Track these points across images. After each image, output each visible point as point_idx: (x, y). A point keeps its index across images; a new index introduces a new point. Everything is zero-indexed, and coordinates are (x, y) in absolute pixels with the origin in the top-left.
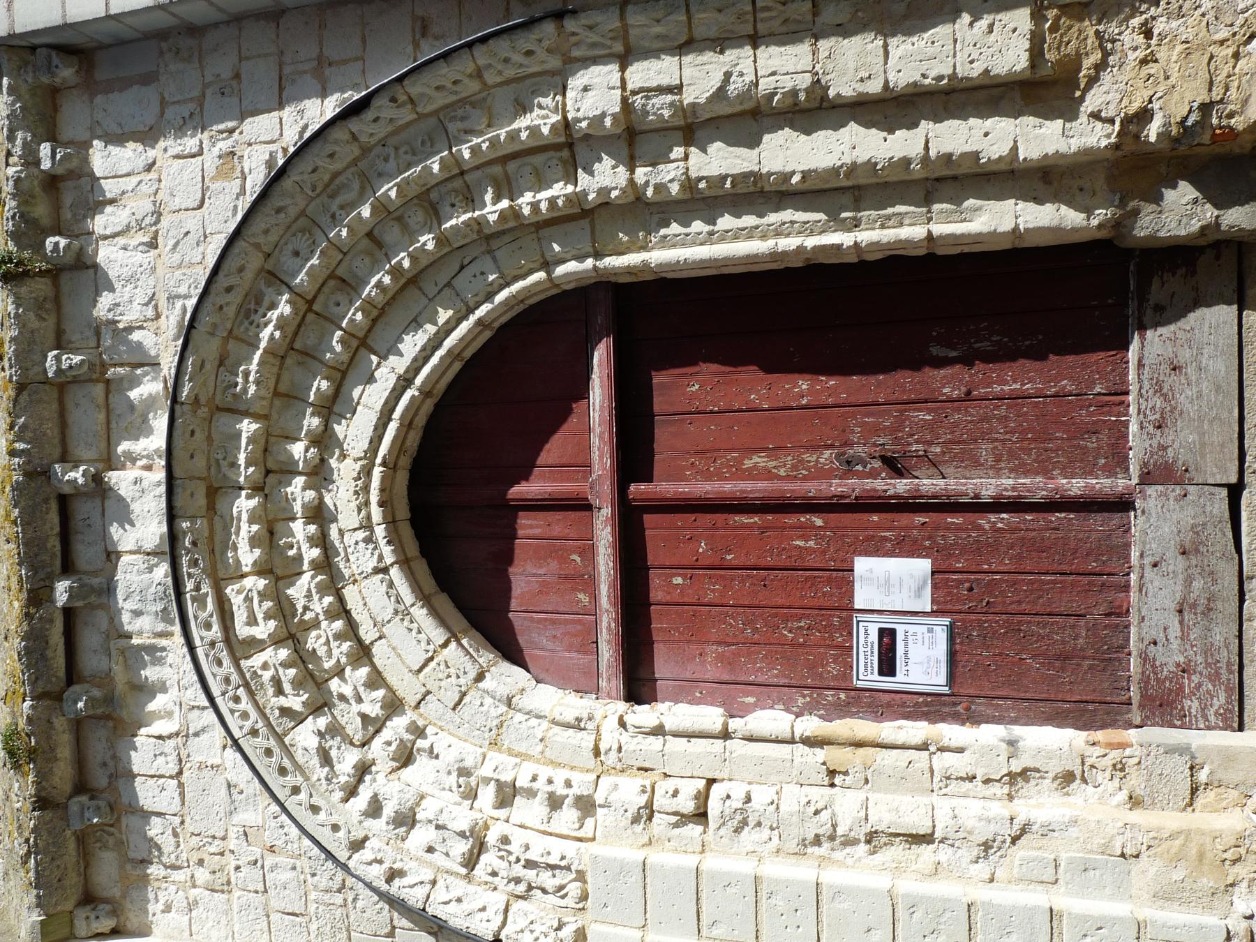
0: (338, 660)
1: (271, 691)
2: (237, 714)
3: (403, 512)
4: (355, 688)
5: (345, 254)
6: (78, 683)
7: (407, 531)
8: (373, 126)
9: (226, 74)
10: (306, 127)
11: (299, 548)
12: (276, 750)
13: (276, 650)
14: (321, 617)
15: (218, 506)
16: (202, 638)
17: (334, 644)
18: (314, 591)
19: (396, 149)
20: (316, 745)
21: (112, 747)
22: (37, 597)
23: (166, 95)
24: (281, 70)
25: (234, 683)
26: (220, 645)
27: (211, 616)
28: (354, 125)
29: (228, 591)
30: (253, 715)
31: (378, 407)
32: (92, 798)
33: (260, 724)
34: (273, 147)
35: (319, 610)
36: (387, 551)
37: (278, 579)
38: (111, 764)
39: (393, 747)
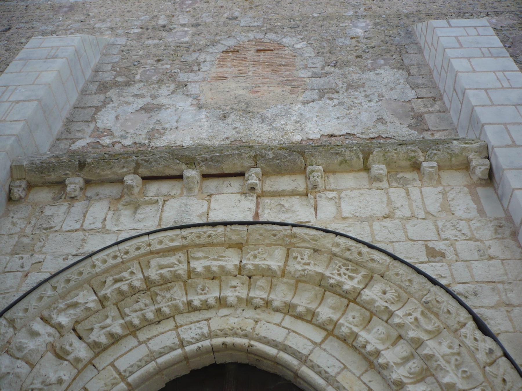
0: (128, 316)
1: (116, 277)
2: (106, 257)
3: (221, 359)
4: (110, 325)
5: (386, 322)
6: (143, 183)
7: (207, 361)
8: (472, 337)
9: (491, 252)
10: (466, 297)
11: (201, 294)
12: (80, 278)
13: (141, 279)
15: (230, 249)
16: (153, 240)
17: (139, 313)
18: (174, 302)
19: (459, 354)
20: (80, 301)
21: (106, 197)
23: (474, 222)
24: (499, 282)
26: (148, 249)
27: (166, 244)
28: (471, 324)
29: (180, 254)
30: (104, 266)
31: (287, 343)
32: (81, 189)
33: (98, 270)
34: (450, 278)
36: (194, 347)
37: (185, 282)
38: (97, 198)
39: (68, 347)
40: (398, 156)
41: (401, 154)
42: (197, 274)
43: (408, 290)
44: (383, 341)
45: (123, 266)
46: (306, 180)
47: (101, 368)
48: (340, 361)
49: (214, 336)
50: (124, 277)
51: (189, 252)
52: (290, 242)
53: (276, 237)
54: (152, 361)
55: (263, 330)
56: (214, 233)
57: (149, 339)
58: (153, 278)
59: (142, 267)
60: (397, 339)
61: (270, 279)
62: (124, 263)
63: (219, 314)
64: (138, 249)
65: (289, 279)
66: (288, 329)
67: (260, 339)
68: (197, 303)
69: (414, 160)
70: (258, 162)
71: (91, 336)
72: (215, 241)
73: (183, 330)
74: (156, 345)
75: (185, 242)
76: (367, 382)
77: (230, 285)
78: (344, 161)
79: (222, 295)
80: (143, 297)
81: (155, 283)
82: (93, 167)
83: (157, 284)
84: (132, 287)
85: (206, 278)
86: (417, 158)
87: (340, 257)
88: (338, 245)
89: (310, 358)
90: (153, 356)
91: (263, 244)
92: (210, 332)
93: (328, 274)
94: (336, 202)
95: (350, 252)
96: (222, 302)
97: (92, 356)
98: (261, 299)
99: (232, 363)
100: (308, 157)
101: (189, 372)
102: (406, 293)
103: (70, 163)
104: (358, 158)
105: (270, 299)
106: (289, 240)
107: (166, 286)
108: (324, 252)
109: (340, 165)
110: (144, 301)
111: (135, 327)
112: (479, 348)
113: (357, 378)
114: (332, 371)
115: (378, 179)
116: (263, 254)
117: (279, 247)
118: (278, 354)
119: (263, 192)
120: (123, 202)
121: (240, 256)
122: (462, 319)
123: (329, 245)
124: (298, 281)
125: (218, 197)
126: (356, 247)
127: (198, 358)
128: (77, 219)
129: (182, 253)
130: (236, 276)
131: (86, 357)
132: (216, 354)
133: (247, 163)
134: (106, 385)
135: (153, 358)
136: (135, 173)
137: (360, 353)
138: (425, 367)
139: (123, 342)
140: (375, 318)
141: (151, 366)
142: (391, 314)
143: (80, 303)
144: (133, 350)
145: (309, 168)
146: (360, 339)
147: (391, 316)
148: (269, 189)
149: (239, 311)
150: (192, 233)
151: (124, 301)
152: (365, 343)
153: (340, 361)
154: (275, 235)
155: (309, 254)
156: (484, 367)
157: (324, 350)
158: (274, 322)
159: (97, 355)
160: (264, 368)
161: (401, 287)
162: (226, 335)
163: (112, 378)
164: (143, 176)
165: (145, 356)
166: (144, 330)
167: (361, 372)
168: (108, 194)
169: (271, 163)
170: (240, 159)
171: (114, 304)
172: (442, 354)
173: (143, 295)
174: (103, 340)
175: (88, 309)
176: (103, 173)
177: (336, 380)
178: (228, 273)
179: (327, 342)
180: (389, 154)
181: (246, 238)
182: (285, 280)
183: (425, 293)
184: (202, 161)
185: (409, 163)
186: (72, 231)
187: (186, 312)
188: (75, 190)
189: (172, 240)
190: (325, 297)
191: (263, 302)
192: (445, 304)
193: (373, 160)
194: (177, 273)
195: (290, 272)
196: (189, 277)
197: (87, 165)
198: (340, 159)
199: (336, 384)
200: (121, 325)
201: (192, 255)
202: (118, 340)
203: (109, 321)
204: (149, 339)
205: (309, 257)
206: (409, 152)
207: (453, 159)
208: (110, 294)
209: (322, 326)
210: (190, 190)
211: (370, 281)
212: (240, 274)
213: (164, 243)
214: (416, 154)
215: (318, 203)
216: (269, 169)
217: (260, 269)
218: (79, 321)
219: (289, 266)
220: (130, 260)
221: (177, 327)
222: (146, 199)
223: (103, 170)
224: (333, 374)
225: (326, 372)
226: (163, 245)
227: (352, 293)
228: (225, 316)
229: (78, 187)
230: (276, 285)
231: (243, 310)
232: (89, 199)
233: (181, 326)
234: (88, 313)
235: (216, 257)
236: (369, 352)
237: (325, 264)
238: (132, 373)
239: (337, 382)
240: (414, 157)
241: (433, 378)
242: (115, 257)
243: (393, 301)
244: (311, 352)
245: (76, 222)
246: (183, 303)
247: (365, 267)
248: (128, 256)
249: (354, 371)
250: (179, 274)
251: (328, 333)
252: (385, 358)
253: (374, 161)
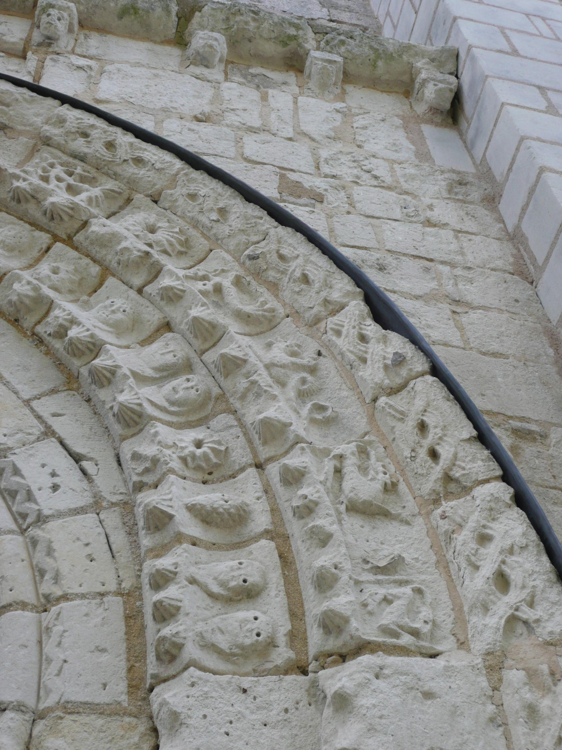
5: (140, 291)
8: (354, 333)
19: (313, 370)
24: (443, 263)
28: (357, 307)
40: (258, 28)
41: (266, 25)
44: (118, 328)
69: (293, 45)
76: (46, 415)
86: (300, 40)
87: (58, 147)
88: (61, 121)
94: (90, 77)
102: (208, 238)
104: (167, 10)
108: (21, 133)
109: (120, 17)
112: (368, 356)
115: (203, 60)
122: (336, 296)
123: (38, 121)
138: (216, 391)
140: (111, 281)
142: (157, 271)
146: (56, 312)
147: (156, 277)
152: (66, 324)
156: (375, 400)
161: (196, 224)
172: (267, 361)
180: (238, 18)
183: (255, 238)
192: (300, 261)
207: (380, 63)
214: (301, 32)
227: (66, 218)
237: (17, 159)
240: (295, 38)
241: (232, 416)
243: (169, 249)
247: (116, 176)
249: (19, 387)
252: (112, 357)
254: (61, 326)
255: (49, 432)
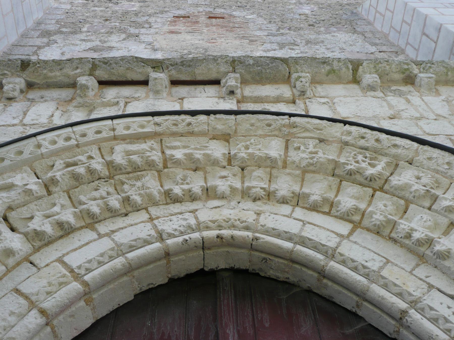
0: (84, 204)
2: (56, 139)
4: (58, 214)
5: (430, 209)
12: (19, 158)
14: (123, 195)
15: (215, 141)
16: (118, 124)
20: (16, 183)
21: (52, 100)
22: (157, 65)
25: (80, 139)
26: (112, 134)
27: (135, 130)
29: (152, 142)
31: (304, 234)
32: (22, 91)
33: (43, 150)
35: (129, 194)
37: (159, 172)
38: (42, 100)
40: (390, 68)
41: (393, 66)
42: (175, 162)
43: (449, 174)
45: (78, 150)
46: (291, 88)
47: (43, 265)
48: (379, 255)
49: (204, 227)
50: (80, 161)
51: (163, 141)
52: (289, 132)
53: (272, 127)
54: (118, 256)
55: (268, 221)
56: (195, 121)
57: (113, 232)
58: (119, 162)
59: (103, 153)
60: (448, 227)
61: (268, 169)
62: (79, 147)
63: (207, 206)
64: (99, 132)
65: (292, 170)
66: (303, 221)
67: (267, 231)
68: (177, 190)
69: (407, 72)
70: (236, 68)
71: (30, 224)
72: (196, 129)
73: (162, 222)
74: (124, 237)
75: (158, 129)
76: (423, 278)
77: (219, 175)
78: (332, 71)
79: (209, 185)
80: (104, 186)
81: (120, 169)
82: (39, 67)
83: (124, 171)
84: (90, 171)
85: (187, 169)
86: (411, 70)
87: (353, 145)
88: (349, 133)
89: (338, 250)
90: (121, 250)
91: (256, 136)
92: (199, 224)
93: (342, 160)
94: (330, 107)
95: (366, 139)
96: (209, 193)
97: (30, 251)
98: (261, 188)
99: (226, 270)
100: (292, 65)
101: (166, 281)
102: (446, 178)
103: (9, 62)
104: (348, 68)
105: (272, 189)
106: (287, 130)
107: (135, 174)
109: (327, 75)
110: (106, 189)
111: (93, 218)
113: (408, 273)
114: (374, 265)
115: (372, 88)
116: (256, 145)
117: (276, 138)
118: (295, 248)
119: (243, 97)
120: (75, 103)
121: (227, 148)
123: (338, 134)
124: (305, 171)
125: (191, 99)
126: (372, 135)
127: (182, 257)
128: (15, 116)
129: (155, 141)
130: (225, 167)
131: (21, 250)
132: (207, 251)
133: (223, 68)
134: (50, 284)
135: (120, 253)
136: (90, 75)
137: (402, 246)
139: (77, 235)
140: (412, 206)
141: (119, 262)
142: (435, 199)
143: (17, 186)
144: (91, 244)
145: (294, 76)
147: (435, 201)
148: (250, 94)
149: (233, 203)
150: (167, 120)
151: (79, 188)
152: (410, 231)
153: (379, 255)
154: (269, 125)
155: (314, 144)
157: (355, 243)
158: (282, 213)
159: (37, 250)
160: (271, 273)
161: (437, 172)
162: (220, 227)
163: (59, 275)
164: (100, 79)
165: (110, 250)
166: (107, 223)
167: (411, 267)
168: (55, 97)
169: (251, 70)
170: (215, 64)
171: (64, 192)
173: (104, 183)
174: (48, 228)
175: (29, 192)
176: (50, 74)
177: (381, 275)
178: (215, 163)
179: (355, 234)
180: (380, 65)
181: (234, 128)
182: (287, 171)
184: (172, 65)
185: (402, 76)
186: (9, 126)
187: (163, 204)
188: (14, 90)
189: (142, 127)
190: (341, 188)
191: (264, 193)
193: (363, 71)
194: (150, 159)
195: (294, 162)
196: (165, 167)
197: (31, 65)
198: (328, 68)
199: (382, 282)
200: (75, 214)
201: (168, 145)
202: (69, 234)
203: (57, 209)
204: (113, 232)
205: (315, 147)
206: (402, 64)
207: (449, 73)
208: (61, 177)
209: (346, 217)
210: (157, 92)
211: (395, 169)
212: (230, 163)
213: (132, 129)
214: (410, 66)
215: (309, 108)
216: (248, 77)
217: (257, 157)
218: (13, 207)
219: (291, 157)
220: (88, 144)
221: (151, 219)
222: (104, 100)
223: (51, 71)
224: (375, 268)
225: (364, 267)
226: (130, 130)
227: (377, 179)
228: (216, 207)
229: (18, 87)
230: (277, 177)
231: (239, 203)
232: (32, 101)
233: (158, 218)
234: (27, 198)
235: (198, 147)
236: (418, 240)
238: (89, 270)
239: (383, 278)
240: (408, 69)
242: (68, 139)
243: (433, 186)
244: (339, 244)
245: (14, 118)
246: (160, 192)
247: (386, 155)
248: (85, 139)
250: (153, 161)
251: (355, 225)
252: (444, 245)
253: (364, 72)
254: (407, 233)
255: (431, 287)
